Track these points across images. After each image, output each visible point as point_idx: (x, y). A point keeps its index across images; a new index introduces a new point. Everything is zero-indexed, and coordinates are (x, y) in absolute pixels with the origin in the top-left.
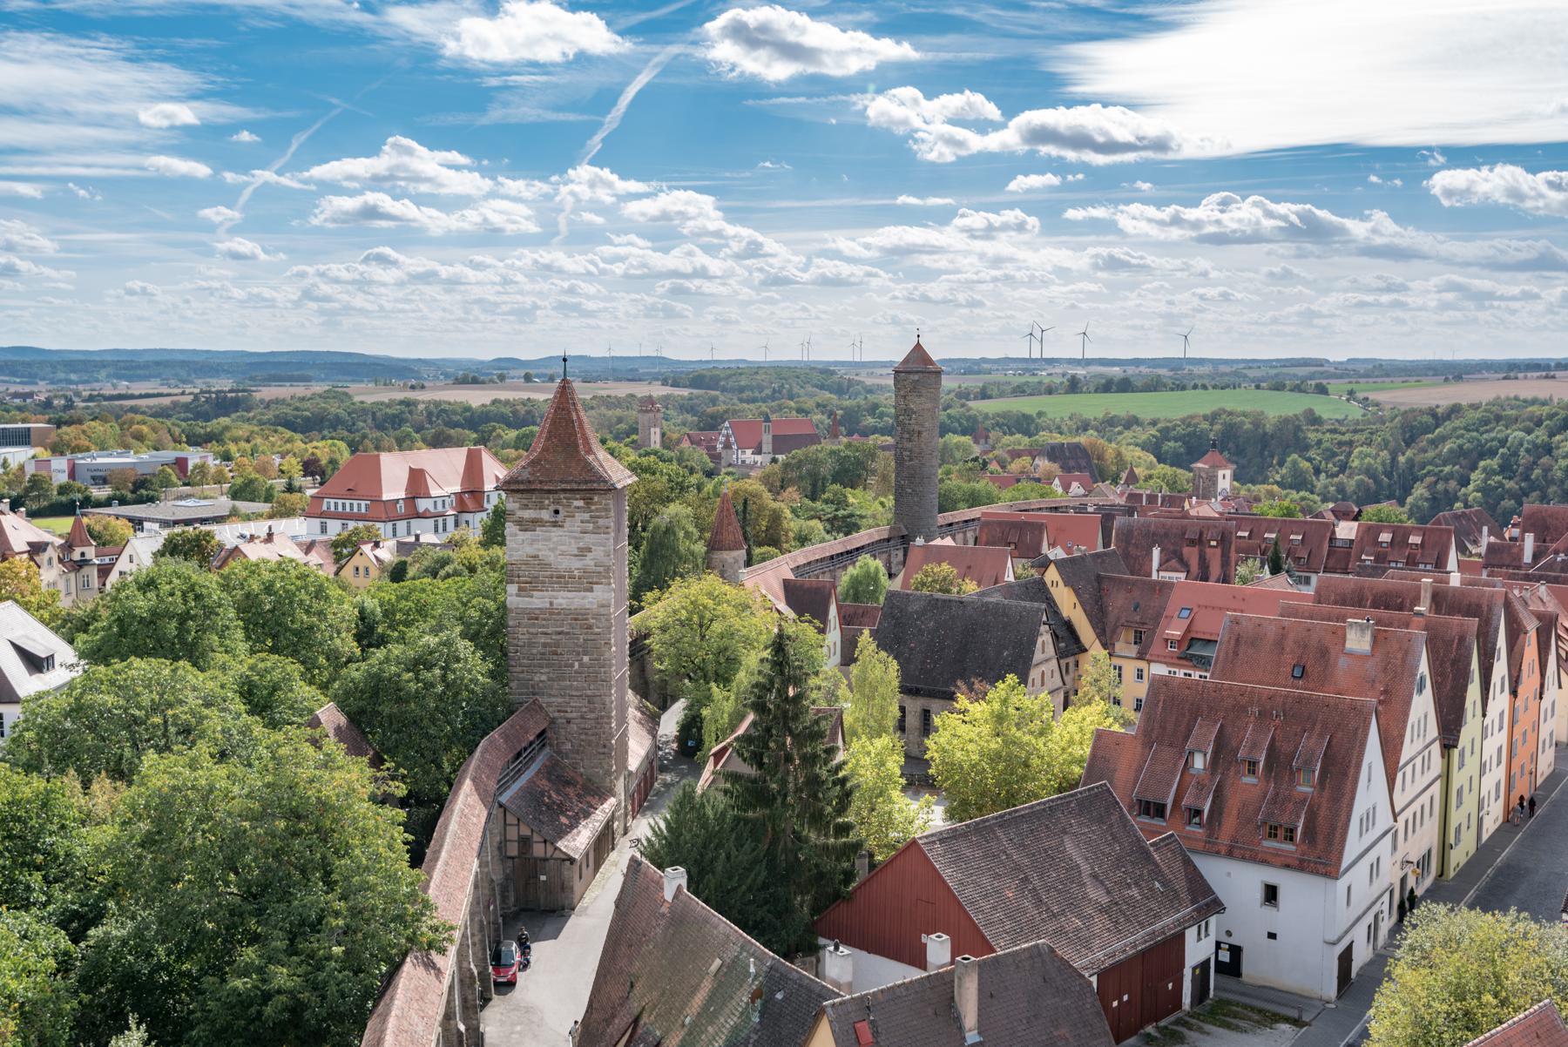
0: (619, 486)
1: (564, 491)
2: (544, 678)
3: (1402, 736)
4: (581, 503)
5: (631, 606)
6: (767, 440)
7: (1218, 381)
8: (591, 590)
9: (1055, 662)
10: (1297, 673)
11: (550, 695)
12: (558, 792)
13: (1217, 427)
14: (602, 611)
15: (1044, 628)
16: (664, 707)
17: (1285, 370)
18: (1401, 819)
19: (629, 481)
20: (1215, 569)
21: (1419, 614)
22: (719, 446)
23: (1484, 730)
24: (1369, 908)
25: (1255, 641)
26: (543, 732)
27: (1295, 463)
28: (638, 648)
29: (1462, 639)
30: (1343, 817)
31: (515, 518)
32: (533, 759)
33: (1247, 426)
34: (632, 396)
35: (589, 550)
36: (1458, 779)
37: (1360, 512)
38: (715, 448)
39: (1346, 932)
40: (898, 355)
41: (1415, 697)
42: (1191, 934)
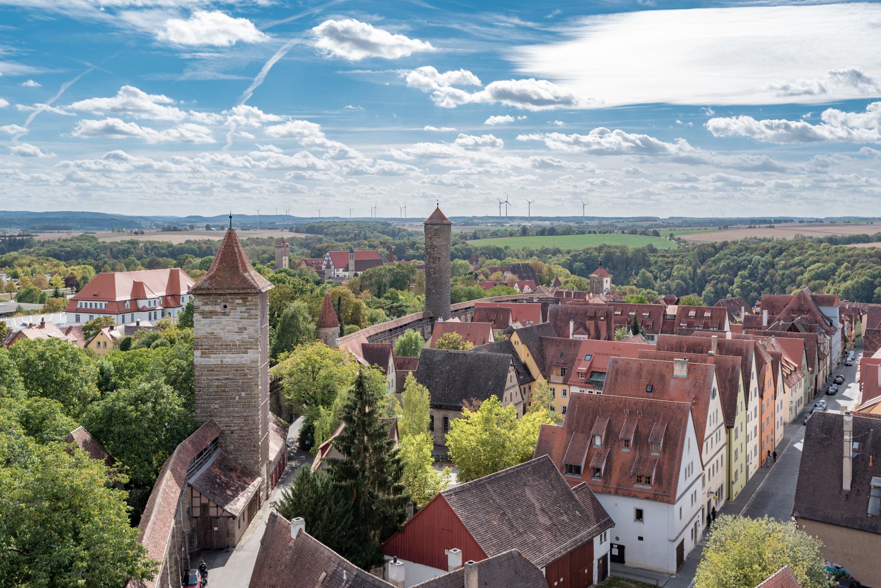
0: (263, 291)
1: (230, 294)
2: (217, 406)
4: (240, 301)
5: (271, 362)
6: (352, 264)
7: (602, 229)
8: (246, 353)
12: (225, 476)
13: (602, 254)
14: (253, 365)
15: (511, 368)
16: (291, 422)
17: (637, 223)
19: (270, 288)
20: (604, 333)
22: (323, 267)
24: (691, 520)
25: (626, 373)
26: (217, 439)
27: (644, 274)
28: (275, 387)
30: (676, 469)
31: (199, 310)
32: (210, 455)
33: (618, 254)
34: (272, 238)
35: (245, 329)
38: (321, 268)
39: (680, 534)
42: (597, 540)
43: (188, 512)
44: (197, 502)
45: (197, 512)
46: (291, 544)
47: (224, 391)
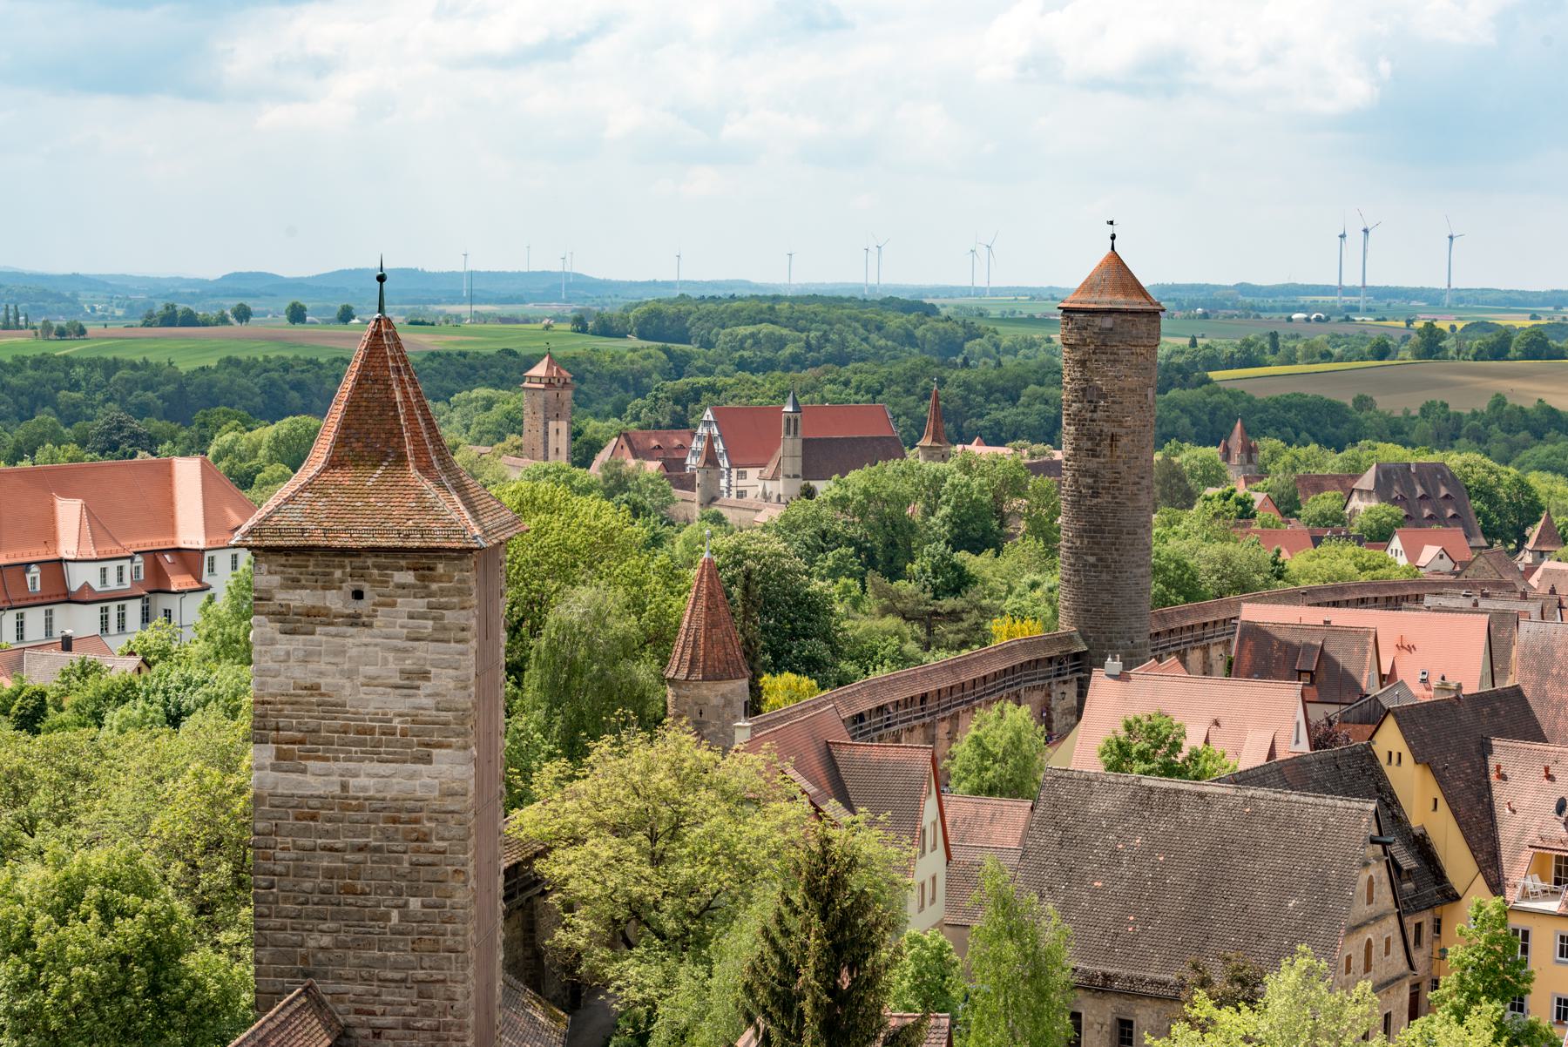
2: (326, 940)
4: (408, 577)
8: (427, 760)
9: (1393, 921)
14: (451, 804)
22: (692, 462)
31: (272, 606)
35: (425, 675)
38: (681, 463)
40: (1067, 271)
47: (351, 891)
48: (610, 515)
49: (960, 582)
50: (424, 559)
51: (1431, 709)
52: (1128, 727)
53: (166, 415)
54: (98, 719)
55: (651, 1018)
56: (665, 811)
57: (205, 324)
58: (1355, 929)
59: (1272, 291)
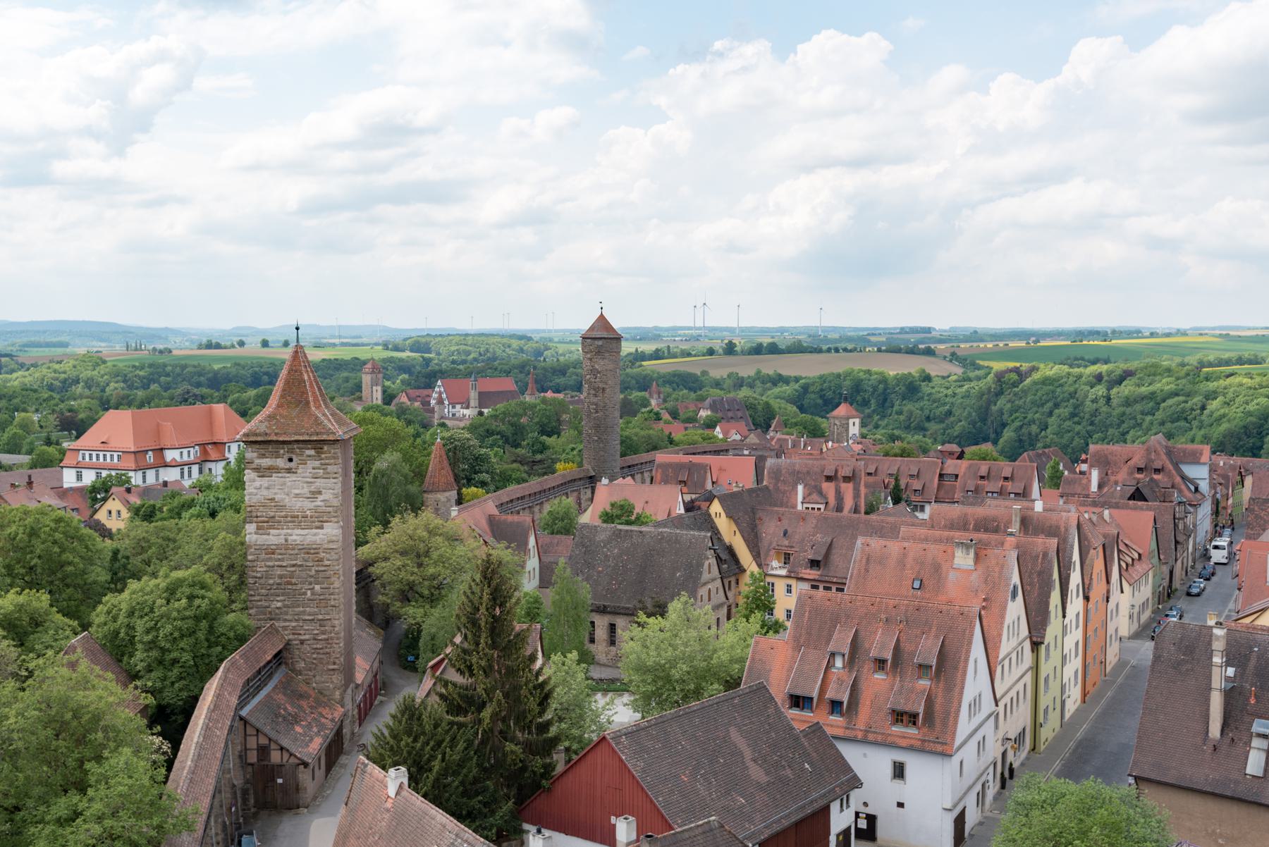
2: (279, 604)
3: (1000, 635)
4: (312, 452)
6: (473, 395)
8: (321, 528)
10: (917, 585)
11: (286, 620)
18: (1001, 704)
21: (1011, 534)
22: (433, 402)
23: (1064, 628)
24: (978, 779)
26: (280, 652)
28: (364, 579)
29: (1045, 555)
30: (955, 704)
31: (254, 466)
32: (270, 676)
35: (320, 493)
36: (1045, 669)
37: (963, 452)
39: (961, 799)
40: (584, 323)
41: (1010, 604)
42: (835, 807)
43: (240, 757)
44: (252, 743)
45: (253, 757)
46: (389, 805)
47: (289, 583)
48: (398, 424)
49: (544, 448)
50: (318, 445)
51: (733, 495)
52: (613, 505)
53: (209, 387)
54: (179, 516)
55: (419, 631)
56: (422, 545)
57: (225, 348)
58: (705, 584)
59: (667, 329)
